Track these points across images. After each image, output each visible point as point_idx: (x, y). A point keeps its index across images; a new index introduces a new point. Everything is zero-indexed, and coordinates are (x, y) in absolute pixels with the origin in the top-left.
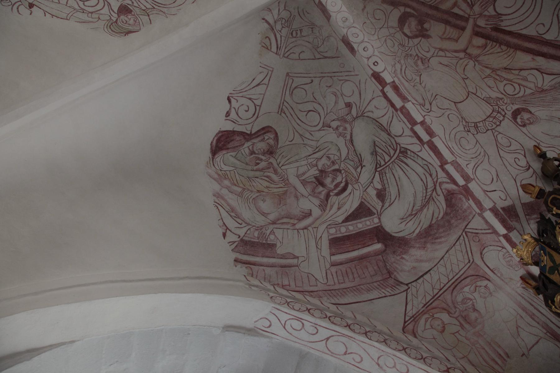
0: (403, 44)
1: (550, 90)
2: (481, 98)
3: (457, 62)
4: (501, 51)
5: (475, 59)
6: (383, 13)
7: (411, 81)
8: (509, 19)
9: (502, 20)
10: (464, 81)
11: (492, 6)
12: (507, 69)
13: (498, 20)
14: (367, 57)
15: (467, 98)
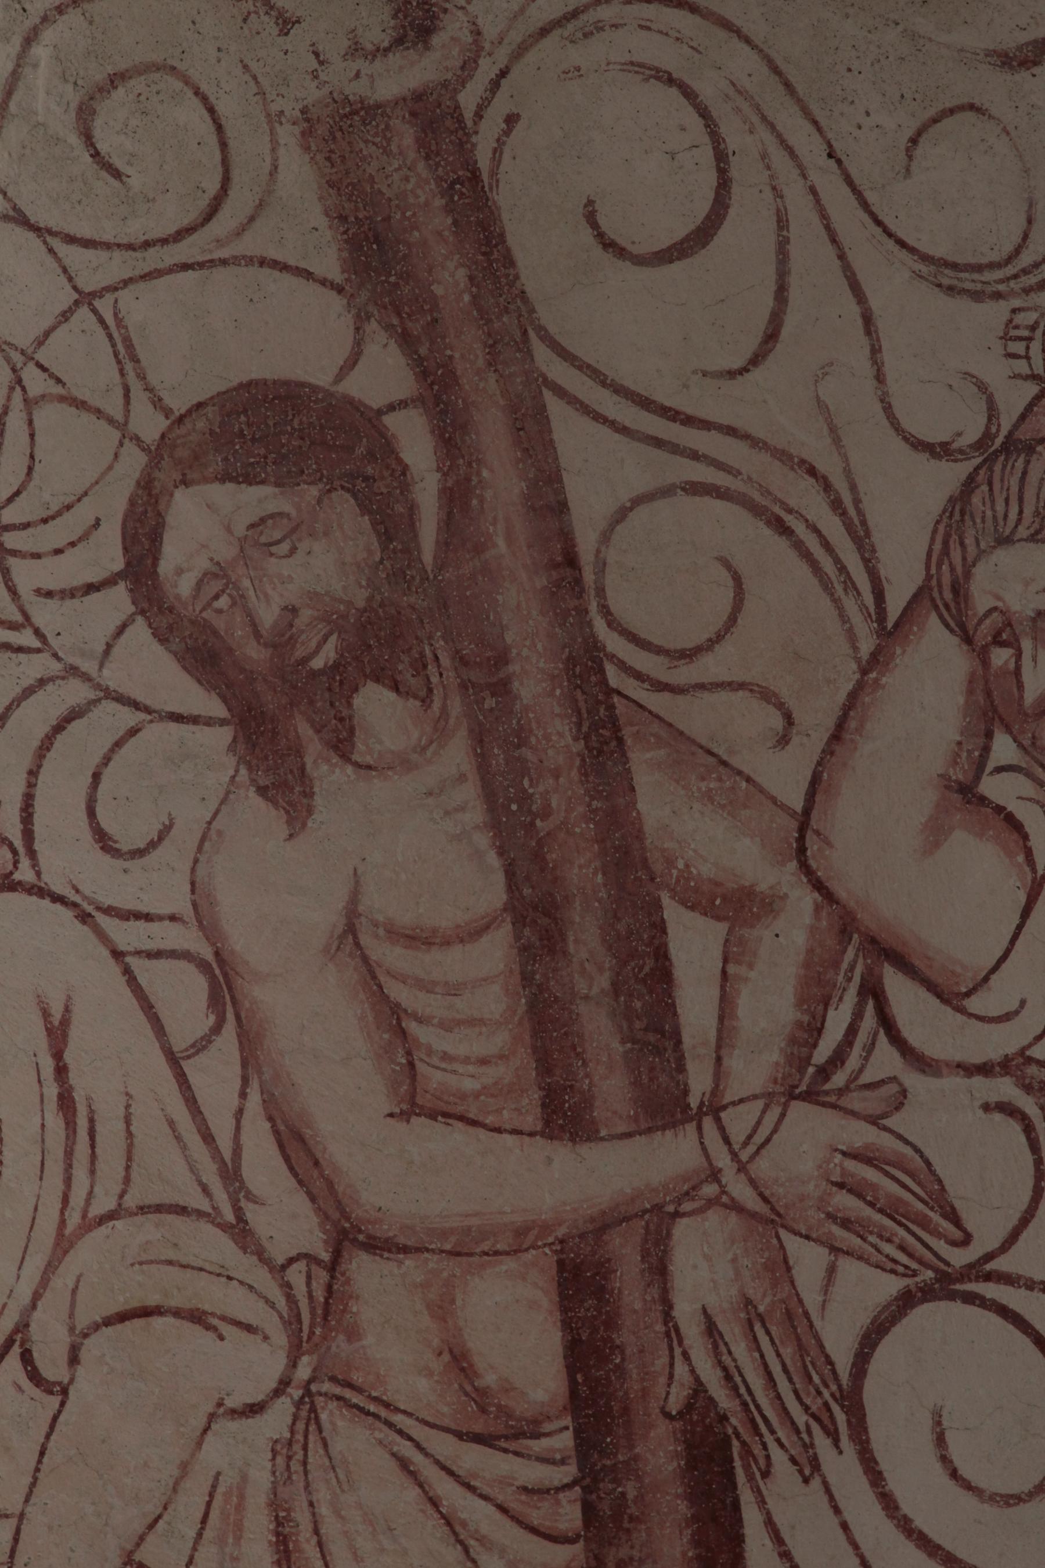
3: (182, 1210)
5: (327, 1387)
6: (213, 186)
8: (845, 1526)
9: (815, 1464)
11: (891, 1286)
13: (801, 1418)
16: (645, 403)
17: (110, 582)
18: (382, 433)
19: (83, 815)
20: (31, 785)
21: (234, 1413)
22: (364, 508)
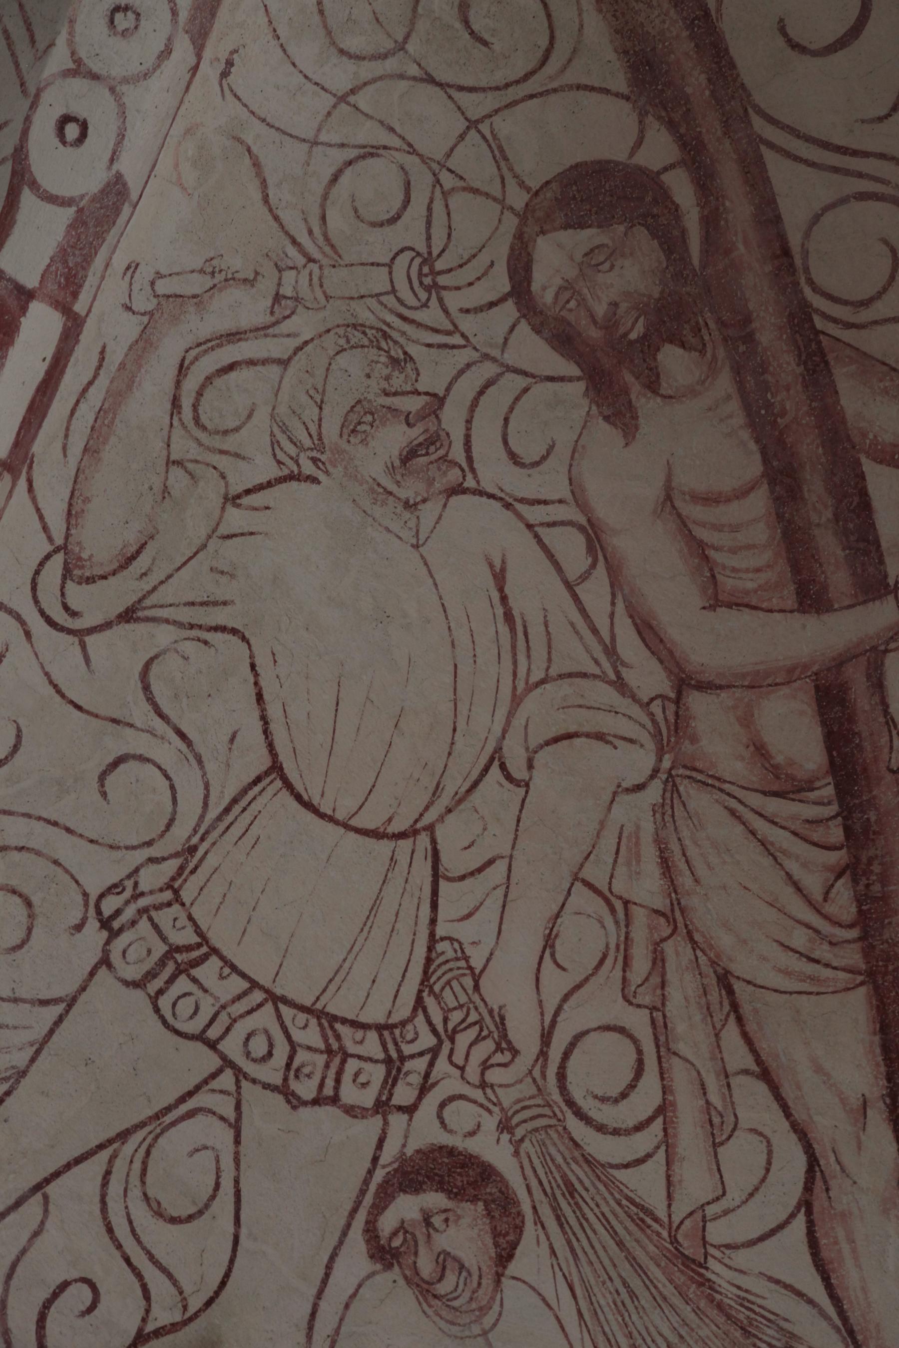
0: (442, 280)
1: (720, 1306)
2: (433, 922)
3: (584, 675)
4: (818, 897)
5: (681, 771)
6: (544, 42)
7: (202, 436)
10: (486, 770)
12: (730, 992)
14: (82, 54)
15: (376, 834)
16: (826, 145)
17: (502, 300)
18: (661, 186)
19: (500, 444)
20: (468, 429)
21: (628, 790)
22: (654, 235)
